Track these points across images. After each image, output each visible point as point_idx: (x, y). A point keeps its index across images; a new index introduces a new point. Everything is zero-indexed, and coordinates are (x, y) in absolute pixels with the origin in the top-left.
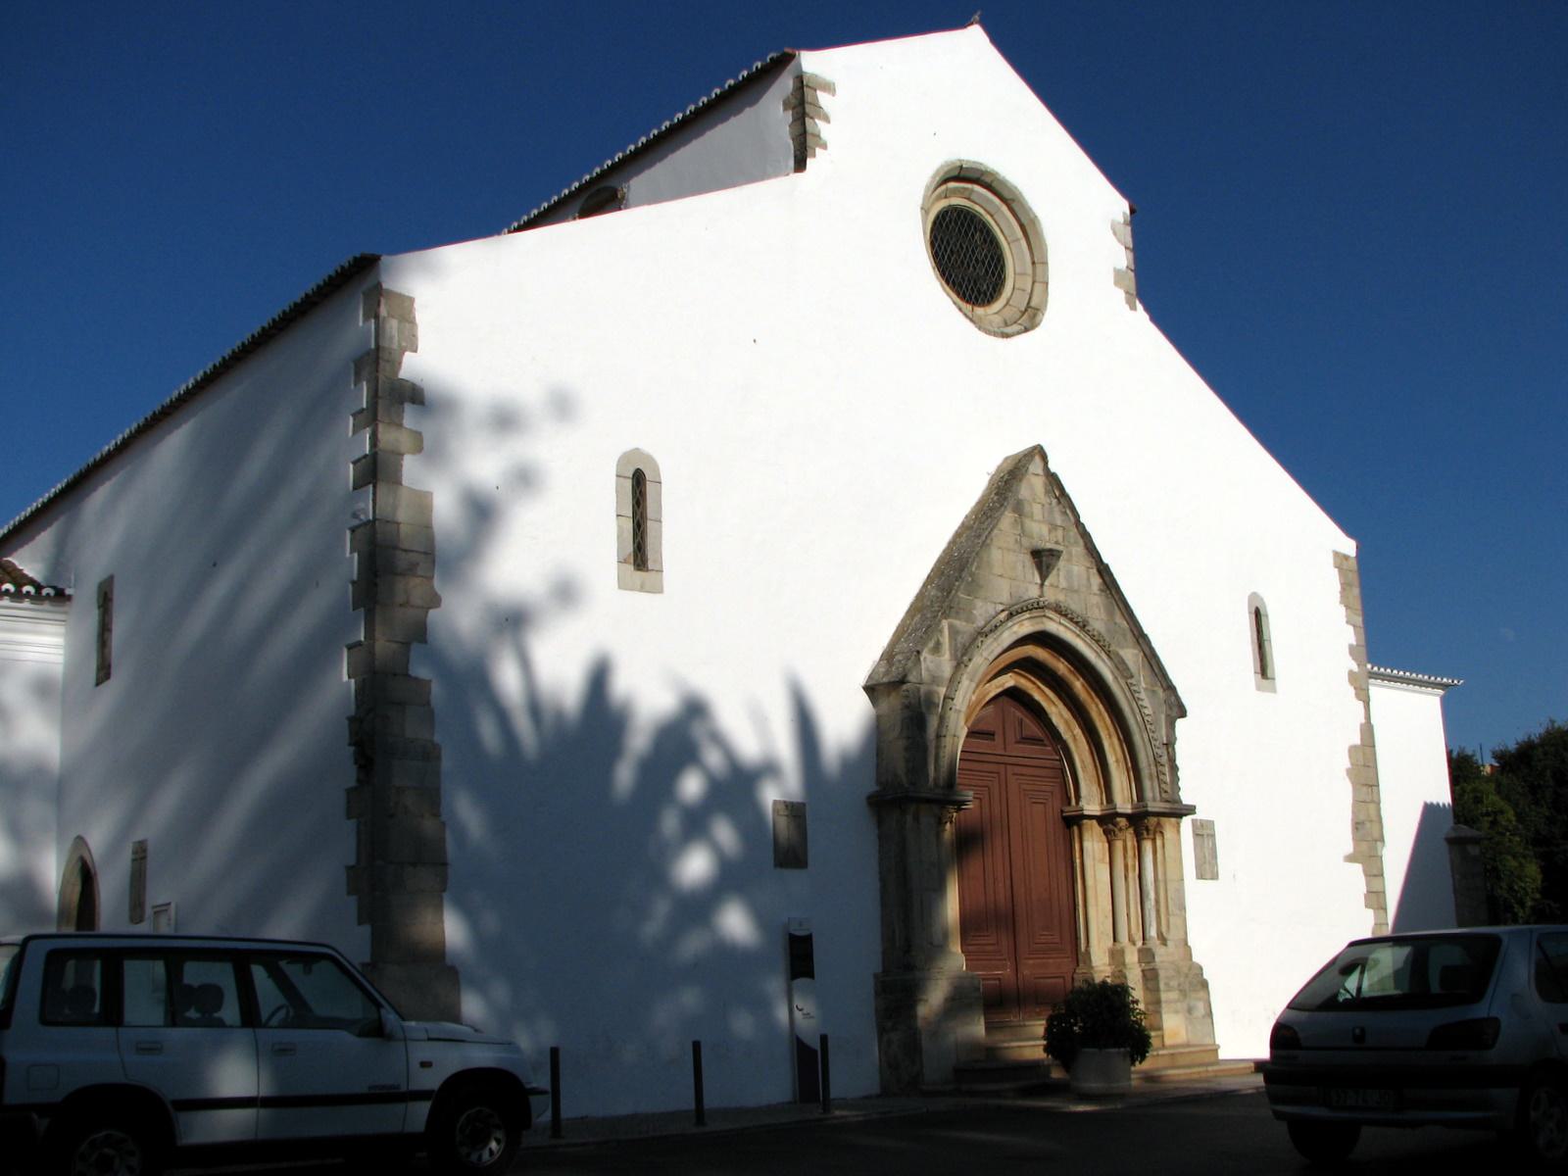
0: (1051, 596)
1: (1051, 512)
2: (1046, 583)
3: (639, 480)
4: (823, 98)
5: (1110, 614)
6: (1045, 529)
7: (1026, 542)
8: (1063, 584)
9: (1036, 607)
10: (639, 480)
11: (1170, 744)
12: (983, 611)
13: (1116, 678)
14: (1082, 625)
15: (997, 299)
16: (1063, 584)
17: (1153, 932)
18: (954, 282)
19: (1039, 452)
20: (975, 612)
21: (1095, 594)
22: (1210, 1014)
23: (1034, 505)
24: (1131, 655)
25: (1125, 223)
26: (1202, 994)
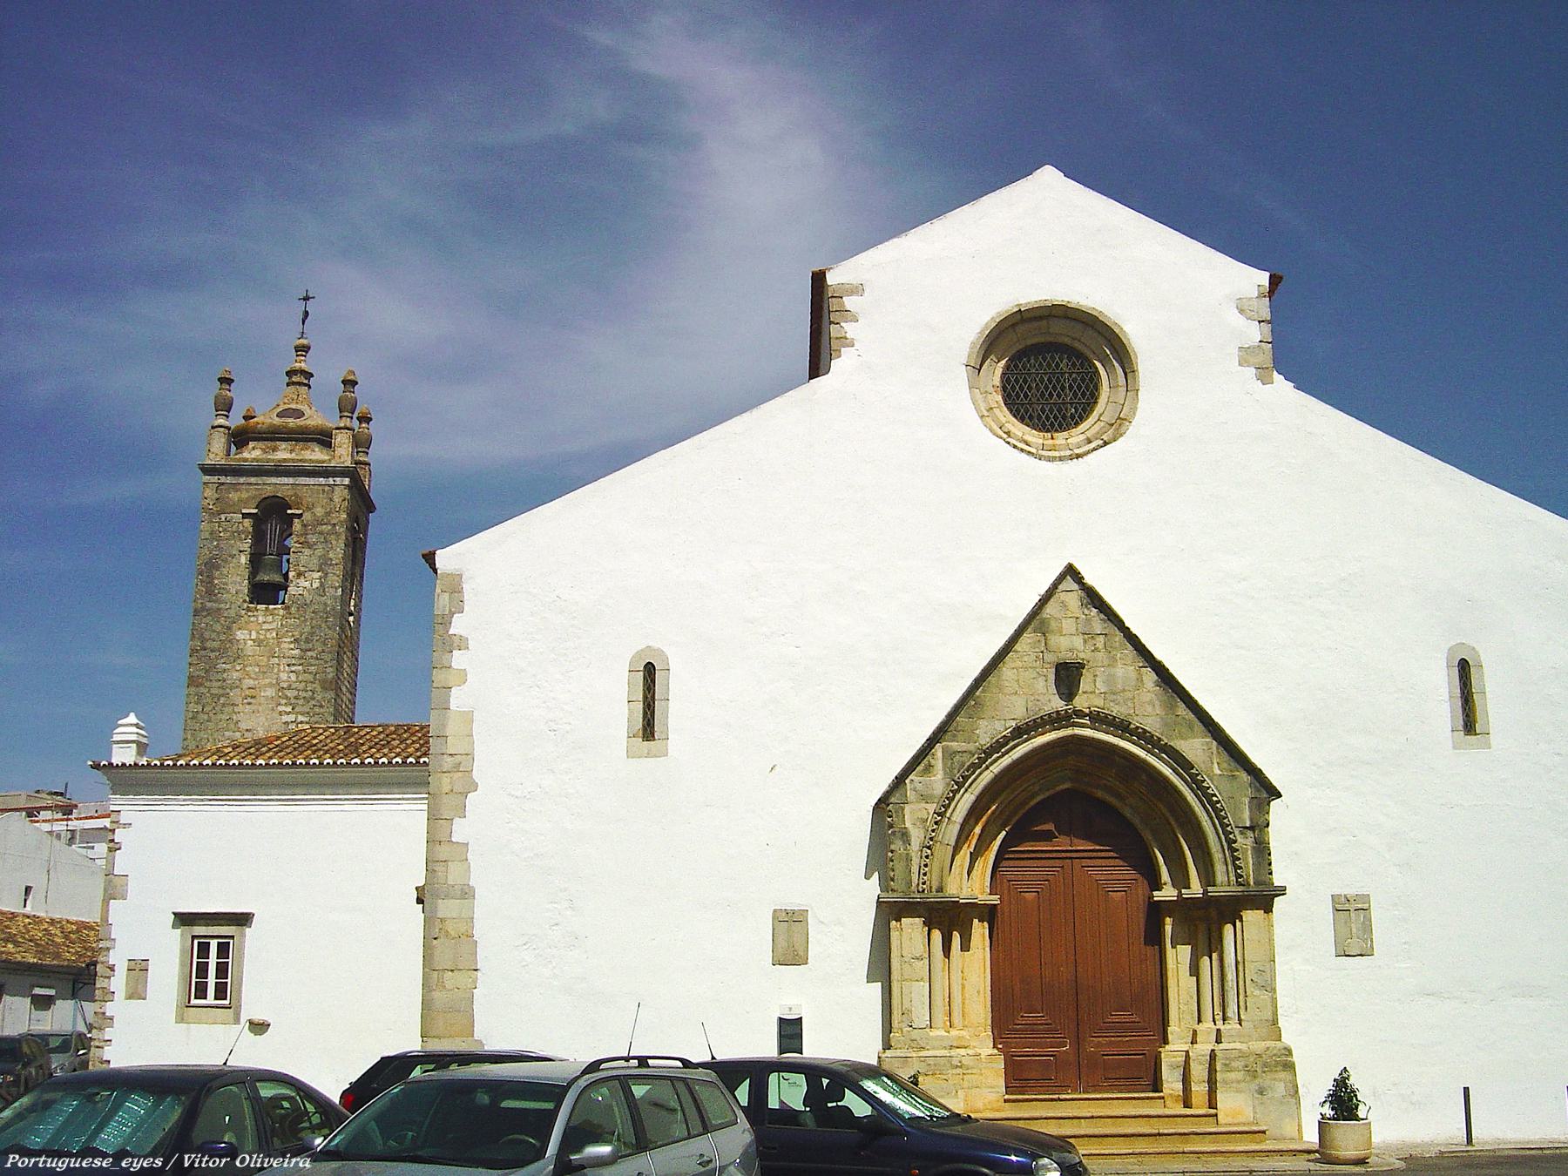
0: (1080, 702)
1: (1088, 621)
3: (650, 670)
4: (849, 302)
5: (1171, 708)
6: (1078, 642)
7: (1050, 657)
9: (1057, 720)
10: (650, 670)
11: (1259, 827)
12: (987, 730)
13: (1174, 770)
14: (1122, 727)
15: (1088, 417)
16: (1101, 687)
18: (1031, 418)
19: (1071, 572)
20: (977, 732)
22: (1295, 1092)
23: (1063, 621)
24: (1195, 748)
25: (1261, 296)
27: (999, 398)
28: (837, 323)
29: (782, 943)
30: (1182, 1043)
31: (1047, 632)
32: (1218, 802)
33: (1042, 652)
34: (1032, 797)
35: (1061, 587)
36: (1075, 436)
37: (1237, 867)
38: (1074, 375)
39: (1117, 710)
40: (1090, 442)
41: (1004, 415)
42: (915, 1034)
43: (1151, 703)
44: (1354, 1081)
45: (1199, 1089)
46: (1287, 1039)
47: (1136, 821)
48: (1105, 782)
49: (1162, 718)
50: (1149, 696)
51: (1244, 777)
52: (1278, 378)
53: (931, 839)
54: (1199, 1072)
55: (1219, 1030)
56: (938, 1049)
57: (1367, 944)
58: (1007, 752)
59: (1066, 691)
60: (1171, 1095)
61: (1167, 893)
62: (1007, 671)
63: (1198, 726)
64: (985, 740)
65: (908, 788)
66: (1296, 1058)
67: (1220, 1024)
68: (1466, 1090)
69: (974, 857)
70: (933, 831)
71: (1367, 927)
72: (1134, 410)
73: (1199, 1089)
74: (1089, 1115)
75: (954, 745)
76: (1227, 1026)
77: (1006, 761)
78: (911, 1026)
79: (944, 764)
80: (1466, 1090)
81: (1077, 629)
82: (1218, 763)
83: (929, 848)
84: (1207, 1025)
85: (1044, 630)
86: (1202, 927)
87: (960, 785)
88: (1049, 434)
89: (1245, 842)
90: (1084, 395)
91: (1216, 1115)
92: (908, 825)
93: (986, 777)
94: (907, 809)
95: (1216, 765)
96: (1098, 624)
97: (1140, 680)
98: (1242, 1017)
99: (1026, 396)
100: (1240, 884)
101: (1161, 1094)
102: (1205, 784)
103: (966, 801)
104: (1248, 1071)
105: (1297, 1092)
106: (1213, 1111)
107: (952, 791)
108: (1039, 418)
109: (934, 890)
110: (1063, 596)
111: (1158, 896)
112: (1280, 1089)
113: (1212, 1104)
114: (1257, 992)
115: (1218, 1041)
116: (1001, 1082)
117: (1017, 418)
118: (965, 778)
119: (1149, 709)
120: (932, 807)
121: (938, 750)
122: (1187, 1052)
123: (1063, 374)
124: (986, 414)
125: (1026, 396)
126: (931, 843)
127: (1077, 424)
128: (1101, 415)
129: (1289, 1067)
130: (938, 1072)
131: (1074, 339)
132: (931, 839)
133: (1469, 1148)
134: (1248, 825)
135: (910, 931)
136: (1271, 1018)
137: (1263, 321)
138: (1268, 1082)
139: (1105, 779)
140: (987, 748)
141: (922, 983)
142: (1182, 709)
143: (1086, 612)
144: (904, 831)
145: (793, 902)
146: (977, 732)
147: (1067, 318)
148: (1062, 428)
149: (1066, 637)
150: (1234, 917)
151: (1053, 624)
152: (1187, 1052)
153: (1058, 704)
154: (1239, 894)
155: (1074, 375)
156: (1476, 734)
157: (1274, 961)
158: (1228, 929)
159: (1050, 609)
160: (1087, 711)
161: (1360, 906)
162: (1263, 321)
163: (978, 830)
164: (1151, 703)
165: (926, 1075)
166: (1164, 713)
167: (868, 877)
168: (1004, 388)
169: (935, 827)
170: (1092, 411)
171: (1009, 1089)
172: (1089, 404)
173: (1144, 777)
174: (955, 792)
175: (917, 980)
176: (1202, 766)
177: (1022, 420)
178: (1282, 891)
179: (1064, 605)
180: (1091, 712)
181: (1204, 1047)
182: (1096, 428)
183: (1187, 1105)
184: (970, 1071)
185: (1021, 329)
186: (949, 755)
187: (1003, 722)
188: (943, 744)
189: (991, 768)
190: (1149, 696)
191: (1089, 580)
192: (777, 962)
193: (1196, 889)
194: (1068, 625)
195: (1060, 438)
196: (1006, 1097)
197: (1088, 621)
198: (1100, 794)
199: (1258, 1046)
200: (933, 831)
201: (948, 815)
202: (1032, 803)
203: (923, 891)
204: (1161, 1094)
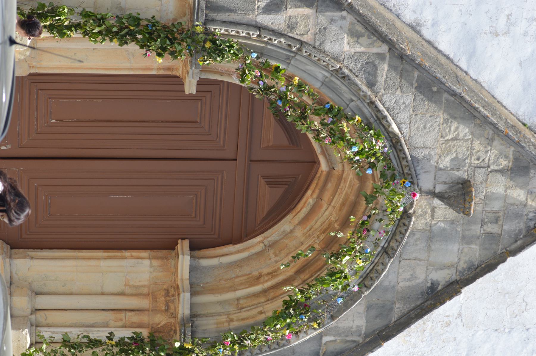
2: (437, 202)
21: (427, 276)
31: (511, 173)
43: (413, 277)
48: (325, 206)
49: (393, 287)
59: (437, 190)
63: (379, 323)
81: (511, 204)
82: (335, 340)
92: (291, 12)
95: (332, 338)
97: (443, 267)
119: (407, 275)
139: (328, 208)
146: (398, 92)
164: (413, 277)
166: (400, 289)
187: (407, 121)
188: (388, 56)
190: (421, 277)
197: (518, 216)
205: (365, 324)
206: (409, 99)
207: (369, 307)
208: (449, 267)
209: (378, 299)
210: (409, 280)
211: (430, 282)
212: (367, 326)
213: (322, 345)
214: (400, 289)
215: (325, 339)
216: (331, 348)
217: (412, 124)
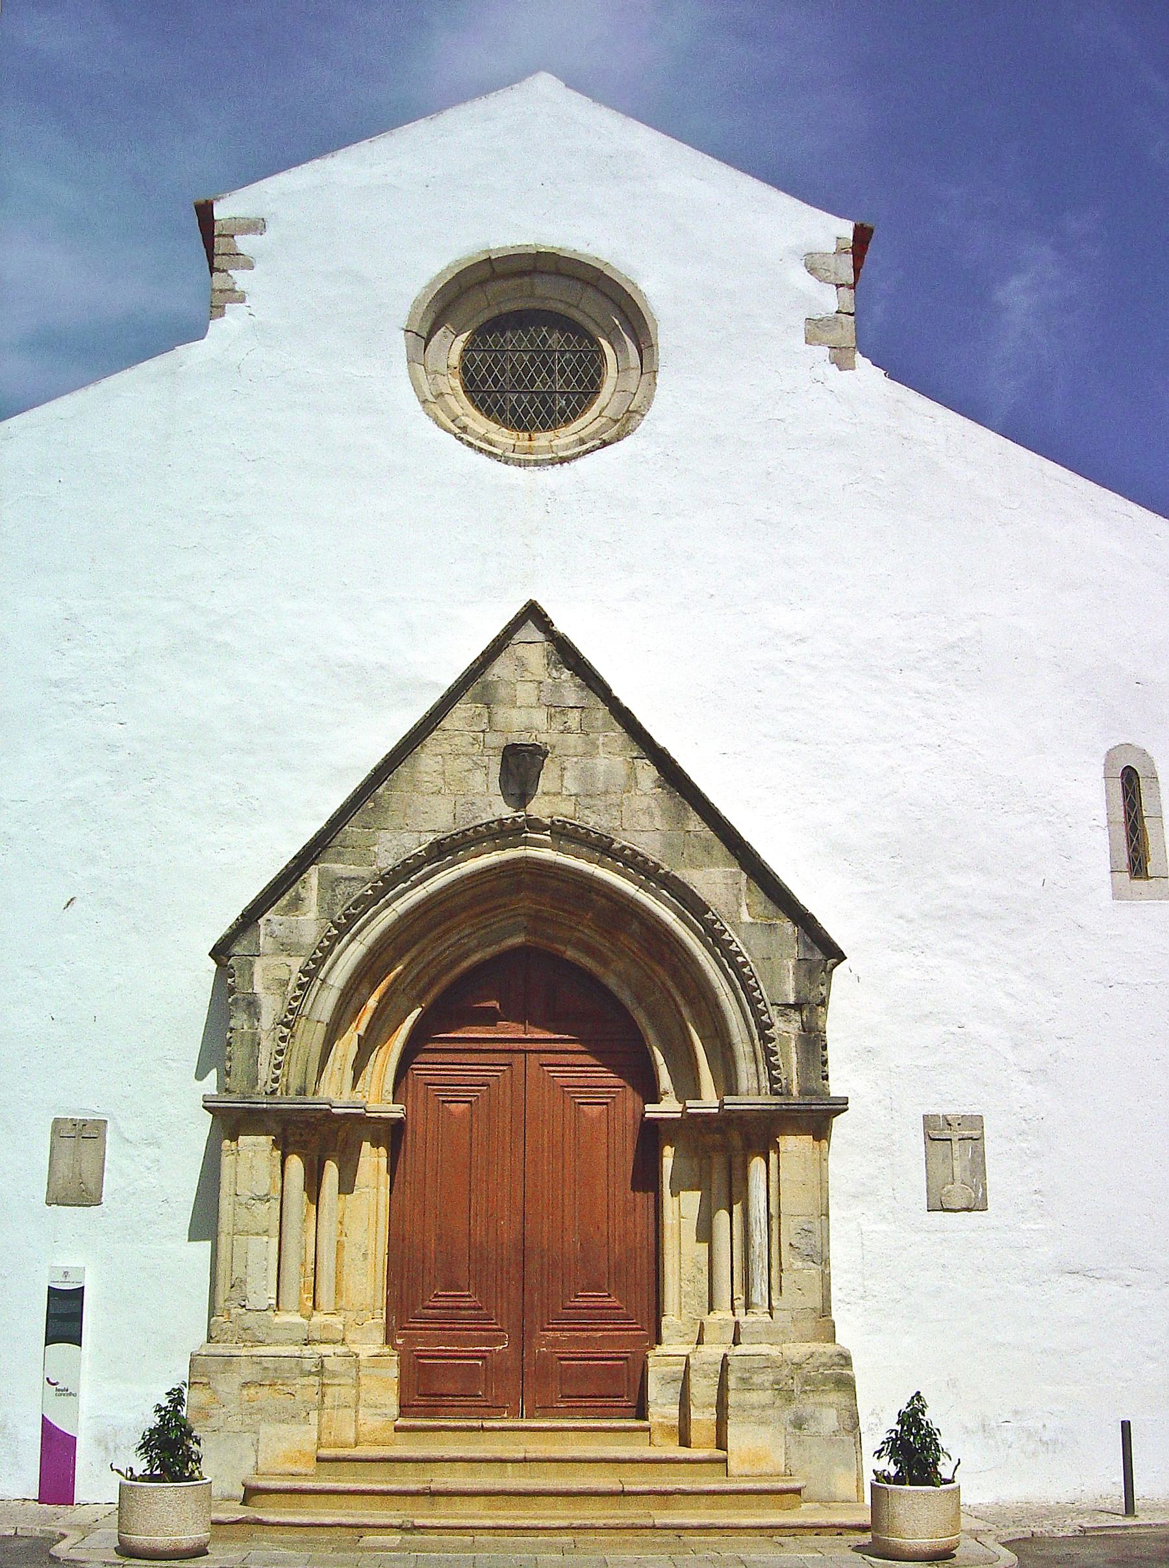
0: (539, 808)
1: (557, 687)
6: (539, 717)
7: (497, 741)
8: (572, 786)
15: (584, 412)
16: (572, 786)
17: (759, 1293)
18: (501, 412)
19: (533, 614)
23: (519, 686)
25: (840, 251)
26: (837, 1397)
27: (456, 383)
28: (224, 271)
29: (63, 1168)
30: (682, 1343)
32: (745, 964)
33: (483, 731)
34: (466, 955)
35: (517, 637)
36: (564, 438)
37: (772, 1067)
38: (568, 355)
39: (593, 821)
40: (584, 443)
41: (462, 406)
42: (250, 1319)
44: (932, 1416)
45: (703, 1417)
46: (845, 1338)
47: (626, 997)
50: (646, 801)
51: (788, 927)
52: (863, 363)
53: (291, 1011)
54: (703, 1390)
55: (737, 1323)
56: (282, 1344)
57: (976, 1192)
58: (421, 881)
60: (661, 1425)
61: (668, 1107)
62: (427, 759)
63: (720, 849)
64: (386, 862)
65: (262, 932)
66: (859, 1371)
67: (740, 1311)
68: (1126, 1427)
69: (367, 1046)
70: (295, 999)
71: (978, 1166)
72: (649, 400)
73: (703, 1417)
74: (521, 1455)
75: (339, 869)
76: (751, 1318)
77: (418, 894)
78: (244, 1306)
79: (321, 899)
80: (1126, 1427)
83: (287, 1025)
84: (723, 1314)
85: (487, 700)
86: (718, 1161)
87: (343, 929)
88: (526, 435)
89: (786, 1029)
90: (580, 382)
91: (725, 1461)
92: (258, 988)
93: (387, 918)
94: (259, 965)
95: (744, 908)
96: (571, 691)
97: (632, 776)
98: (774, 1303)
99: (496, 381)
100: (776, 1093)
101: (645, 1424)
102: (726, 937)
103: (352, 953)
104: (779, 1390)
105: (856, 1425)
106: (720, 1454)
107: (329, 938)
108: (513, 411)
109: (292, 1091)
110: (520, 650)
111: (652, 1110)
112: (829, 1419)
113: (721, 1444)
114: (799, 1264)
115: (736, 1342)
116: (391, 1400)
117: (480, 410)
118: (351, 919)
119: (645, 820)
120: (297, 963)
121: (313, 875)
122: (688, 1357)
123: (551, 352)
124: (431, 398)
125: (496, 381)
126: (290, 1017)
127: (568, 421)
128: (603, 409)
129: (846, 1384)
130: (280, 1382)
131: (571, 305)
132: (291, 1011)
133: (1129, 1521)
134: (792, 1000)
135: (251, 1154)
136: (819, 1306)
137: (842, 285)
138: (809, 1409)
140: (388, 874)
141: (265, 1239)
142: (695, 823)
143: (555, 674)
144: (250, 998)
145: (82, 1107)
146: (376, 849)
147: (558, 273)
148: (545, 427)
149: (523, 711)
150: (766, 1145)
151: (503, 692)
152: (688, 1357)
153: (506, 812)
154: (773, 1107)
155: (568, 355)
156: (1148, 878)
157: (827, 1215)
158: (757, 1164)
159: (500, 669)
160: (548, 821)
161: (967, 1133)
162: (842, 285)
163: (372, 1002)
164: (648, 812)
165: (260, 1385)
166: (667, 827)
167: (200, 1075)
168: (465, 370)
169: (298, 993)
170: (591, 403)
171: (405, 1409)
172: (586, 395)
173: (635, 926)
174: (336, 939)
175: (257, 1234)
176: (723, 909)
177: (488, 414)
178: (840, 1106)
179: (522, 664)
180: (553, 822)
181: (713, 1351)
182: (596, 424)
183: (685, 1442)
184: (336, 1381)
185: (494, 288)
186: (330, 883)
187: (416, 835)
188: (321, 865)
189: (394, 906)
191: (561, 626)
192: (55, 1198)
193: (709, 1099)
194: (526, 693)
195: (542, 439)
196: (401, 1422)
198: (570, 953)
199: (797, 1350)
200: (295, 999)
201: (322, 976)
202: (466, 964)
203: (273, 1092)
204: (645, 1424)
205: (722, 869)
206: (384, 836)
207: (694, 864)
208: (633, 768)
209: (683, 853)
210: (652, 816)
211: (654, 791)
212: (725, 865)
213: (755, 921)
214: (667, 827)
215: (746, 918)
216: (759, 909)
217: (421, 829)
